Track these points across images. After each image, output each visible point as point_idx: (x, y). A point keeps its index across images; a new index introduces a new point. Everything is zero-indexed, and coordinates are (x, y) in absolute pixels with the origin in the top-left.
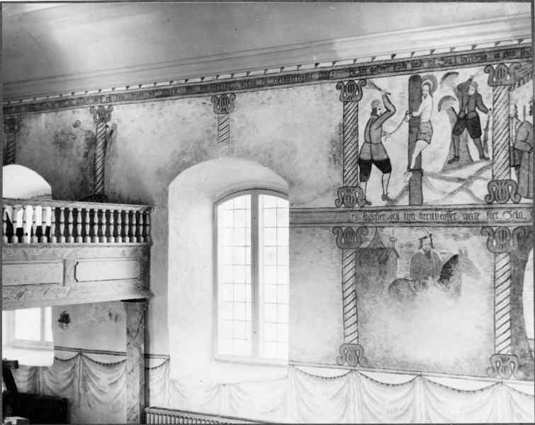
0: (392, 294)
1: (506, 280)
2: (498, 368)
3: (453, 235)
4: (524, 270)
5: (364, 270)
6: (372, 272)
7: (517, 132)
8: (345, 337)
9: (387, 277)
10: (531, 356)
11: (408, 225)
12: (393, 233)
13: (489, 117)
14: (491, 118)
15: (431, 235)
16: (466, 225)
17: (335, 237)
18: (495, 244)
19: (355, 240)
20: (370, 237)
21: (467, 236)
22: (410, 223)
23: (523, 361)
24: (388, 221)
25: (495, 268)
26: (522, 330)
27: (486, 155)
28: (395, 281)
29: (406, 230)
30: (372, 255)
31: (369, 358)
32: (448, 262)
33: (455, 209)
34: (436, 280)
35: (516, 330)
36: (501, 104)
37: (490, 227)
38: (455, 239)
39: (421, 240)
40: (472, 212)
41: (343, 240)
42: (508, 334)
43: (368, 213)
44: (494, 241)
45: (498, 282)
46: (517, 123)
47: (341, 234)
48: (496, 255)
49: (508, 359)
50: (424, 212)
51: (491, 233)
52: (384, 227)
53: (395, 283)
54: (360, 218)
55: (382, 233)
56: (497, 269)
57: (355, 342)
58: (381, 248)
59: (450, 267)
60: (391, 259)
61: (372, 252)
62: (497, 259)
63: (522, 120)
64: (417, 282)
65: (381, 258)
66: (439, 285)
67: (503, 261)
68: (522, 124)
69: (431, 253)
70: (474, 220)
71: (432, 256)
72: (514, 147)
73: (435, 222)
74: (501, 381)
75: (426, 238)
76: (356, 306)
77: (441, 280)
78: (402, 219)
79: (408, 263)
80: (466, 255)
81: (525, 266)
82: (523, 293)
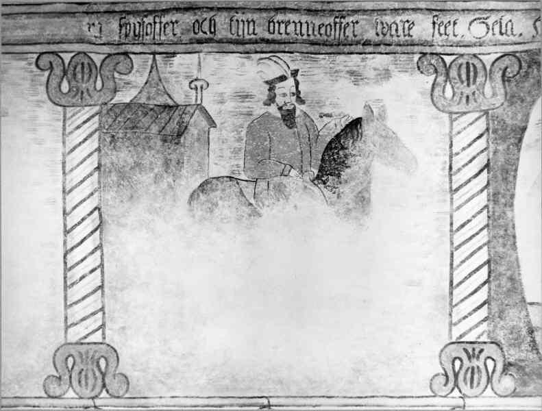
0: (199, 213)
1: (477, 175)
2: (456, 375)
3: (352, 73)
4: (519, 150)
5: (124, 156)
6: (146, 162)
8: (67, 328)
9: (184, 171)
10: (534, 341)
11: (241, 48)
12: (199, 69)
15: (295, 73)
16: (382, 48)
17: (44, 79)
18: (449, 92)
19: (99, 84)
20: (138, 78)
21: (386, 74)
22: (243, 43)
23: (513, 355)
24: (185, 38)
25: (451, 146)
26: (515, 284)
28: (206, 183)
29: (232, 61)
30: (146, 121)
31: (133, 375)
32: (338, 136)
33: (355, 12)
34: (307, 178)
35: (499, 286)
37: (436, 54)
38: (356, 83)
39: (271, 84)
40: (398, 19)
41: (65, 87)
42: (482, 295)
43: (132, 20)
44: (448, 87)
45: (459, 179)
47: (58, 71)
48: (453, 116)
49: (481, 351)
50: (280, 17)
51: (441, 69)
52: (174, 54)
53: (203, 187)
54: (111, 31)
55: (169, 69)
56: (455, 150)
57: (97, 337)
58: (166, 107)
59: (343, 148)
60: (193, 131)
61: (146, 114)
62: (457, 126)
64: (262, 185)
65: (168, 128)
66: (316, 189)
67: (471, 128)
69: (298, 113)
70: (402, 38)
71: (299, 120)
73: (304, 42)
74: (461, 402)
75: (282, 78)
76: (99, 247)
77: (320, 179)
78: (222, 33)
79: (240, 140)
80: (382, 117)
81: (520, 140)
82: (516, 202)
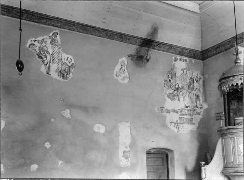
7: (62, 66)
13: (51, 57)
14: (52, 58)
27: (49, 73)
36: (56, 53)
46: (62, 62)
63: (64, 62)
68: (64, 63)
72: (60, 72)
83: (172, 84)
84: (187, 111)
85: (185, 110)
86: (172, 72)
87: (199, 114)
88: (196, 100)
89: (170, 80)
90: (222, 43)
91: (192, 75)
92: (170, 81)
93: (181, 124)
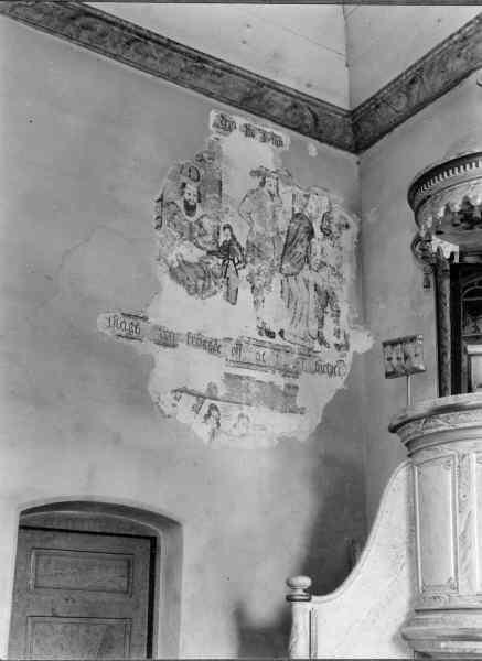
83: (201, 226)
84: (268, 351)
85: (260, 344)
86: (202, 172)
87: (332, 371)
88: (316, 310)
89: (191, 203)
90: (431, 56)
91: (305, 206)
92: (190, 209)
93: (235, 407)
